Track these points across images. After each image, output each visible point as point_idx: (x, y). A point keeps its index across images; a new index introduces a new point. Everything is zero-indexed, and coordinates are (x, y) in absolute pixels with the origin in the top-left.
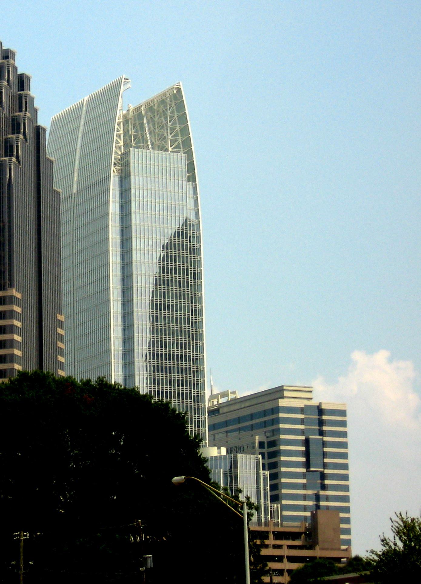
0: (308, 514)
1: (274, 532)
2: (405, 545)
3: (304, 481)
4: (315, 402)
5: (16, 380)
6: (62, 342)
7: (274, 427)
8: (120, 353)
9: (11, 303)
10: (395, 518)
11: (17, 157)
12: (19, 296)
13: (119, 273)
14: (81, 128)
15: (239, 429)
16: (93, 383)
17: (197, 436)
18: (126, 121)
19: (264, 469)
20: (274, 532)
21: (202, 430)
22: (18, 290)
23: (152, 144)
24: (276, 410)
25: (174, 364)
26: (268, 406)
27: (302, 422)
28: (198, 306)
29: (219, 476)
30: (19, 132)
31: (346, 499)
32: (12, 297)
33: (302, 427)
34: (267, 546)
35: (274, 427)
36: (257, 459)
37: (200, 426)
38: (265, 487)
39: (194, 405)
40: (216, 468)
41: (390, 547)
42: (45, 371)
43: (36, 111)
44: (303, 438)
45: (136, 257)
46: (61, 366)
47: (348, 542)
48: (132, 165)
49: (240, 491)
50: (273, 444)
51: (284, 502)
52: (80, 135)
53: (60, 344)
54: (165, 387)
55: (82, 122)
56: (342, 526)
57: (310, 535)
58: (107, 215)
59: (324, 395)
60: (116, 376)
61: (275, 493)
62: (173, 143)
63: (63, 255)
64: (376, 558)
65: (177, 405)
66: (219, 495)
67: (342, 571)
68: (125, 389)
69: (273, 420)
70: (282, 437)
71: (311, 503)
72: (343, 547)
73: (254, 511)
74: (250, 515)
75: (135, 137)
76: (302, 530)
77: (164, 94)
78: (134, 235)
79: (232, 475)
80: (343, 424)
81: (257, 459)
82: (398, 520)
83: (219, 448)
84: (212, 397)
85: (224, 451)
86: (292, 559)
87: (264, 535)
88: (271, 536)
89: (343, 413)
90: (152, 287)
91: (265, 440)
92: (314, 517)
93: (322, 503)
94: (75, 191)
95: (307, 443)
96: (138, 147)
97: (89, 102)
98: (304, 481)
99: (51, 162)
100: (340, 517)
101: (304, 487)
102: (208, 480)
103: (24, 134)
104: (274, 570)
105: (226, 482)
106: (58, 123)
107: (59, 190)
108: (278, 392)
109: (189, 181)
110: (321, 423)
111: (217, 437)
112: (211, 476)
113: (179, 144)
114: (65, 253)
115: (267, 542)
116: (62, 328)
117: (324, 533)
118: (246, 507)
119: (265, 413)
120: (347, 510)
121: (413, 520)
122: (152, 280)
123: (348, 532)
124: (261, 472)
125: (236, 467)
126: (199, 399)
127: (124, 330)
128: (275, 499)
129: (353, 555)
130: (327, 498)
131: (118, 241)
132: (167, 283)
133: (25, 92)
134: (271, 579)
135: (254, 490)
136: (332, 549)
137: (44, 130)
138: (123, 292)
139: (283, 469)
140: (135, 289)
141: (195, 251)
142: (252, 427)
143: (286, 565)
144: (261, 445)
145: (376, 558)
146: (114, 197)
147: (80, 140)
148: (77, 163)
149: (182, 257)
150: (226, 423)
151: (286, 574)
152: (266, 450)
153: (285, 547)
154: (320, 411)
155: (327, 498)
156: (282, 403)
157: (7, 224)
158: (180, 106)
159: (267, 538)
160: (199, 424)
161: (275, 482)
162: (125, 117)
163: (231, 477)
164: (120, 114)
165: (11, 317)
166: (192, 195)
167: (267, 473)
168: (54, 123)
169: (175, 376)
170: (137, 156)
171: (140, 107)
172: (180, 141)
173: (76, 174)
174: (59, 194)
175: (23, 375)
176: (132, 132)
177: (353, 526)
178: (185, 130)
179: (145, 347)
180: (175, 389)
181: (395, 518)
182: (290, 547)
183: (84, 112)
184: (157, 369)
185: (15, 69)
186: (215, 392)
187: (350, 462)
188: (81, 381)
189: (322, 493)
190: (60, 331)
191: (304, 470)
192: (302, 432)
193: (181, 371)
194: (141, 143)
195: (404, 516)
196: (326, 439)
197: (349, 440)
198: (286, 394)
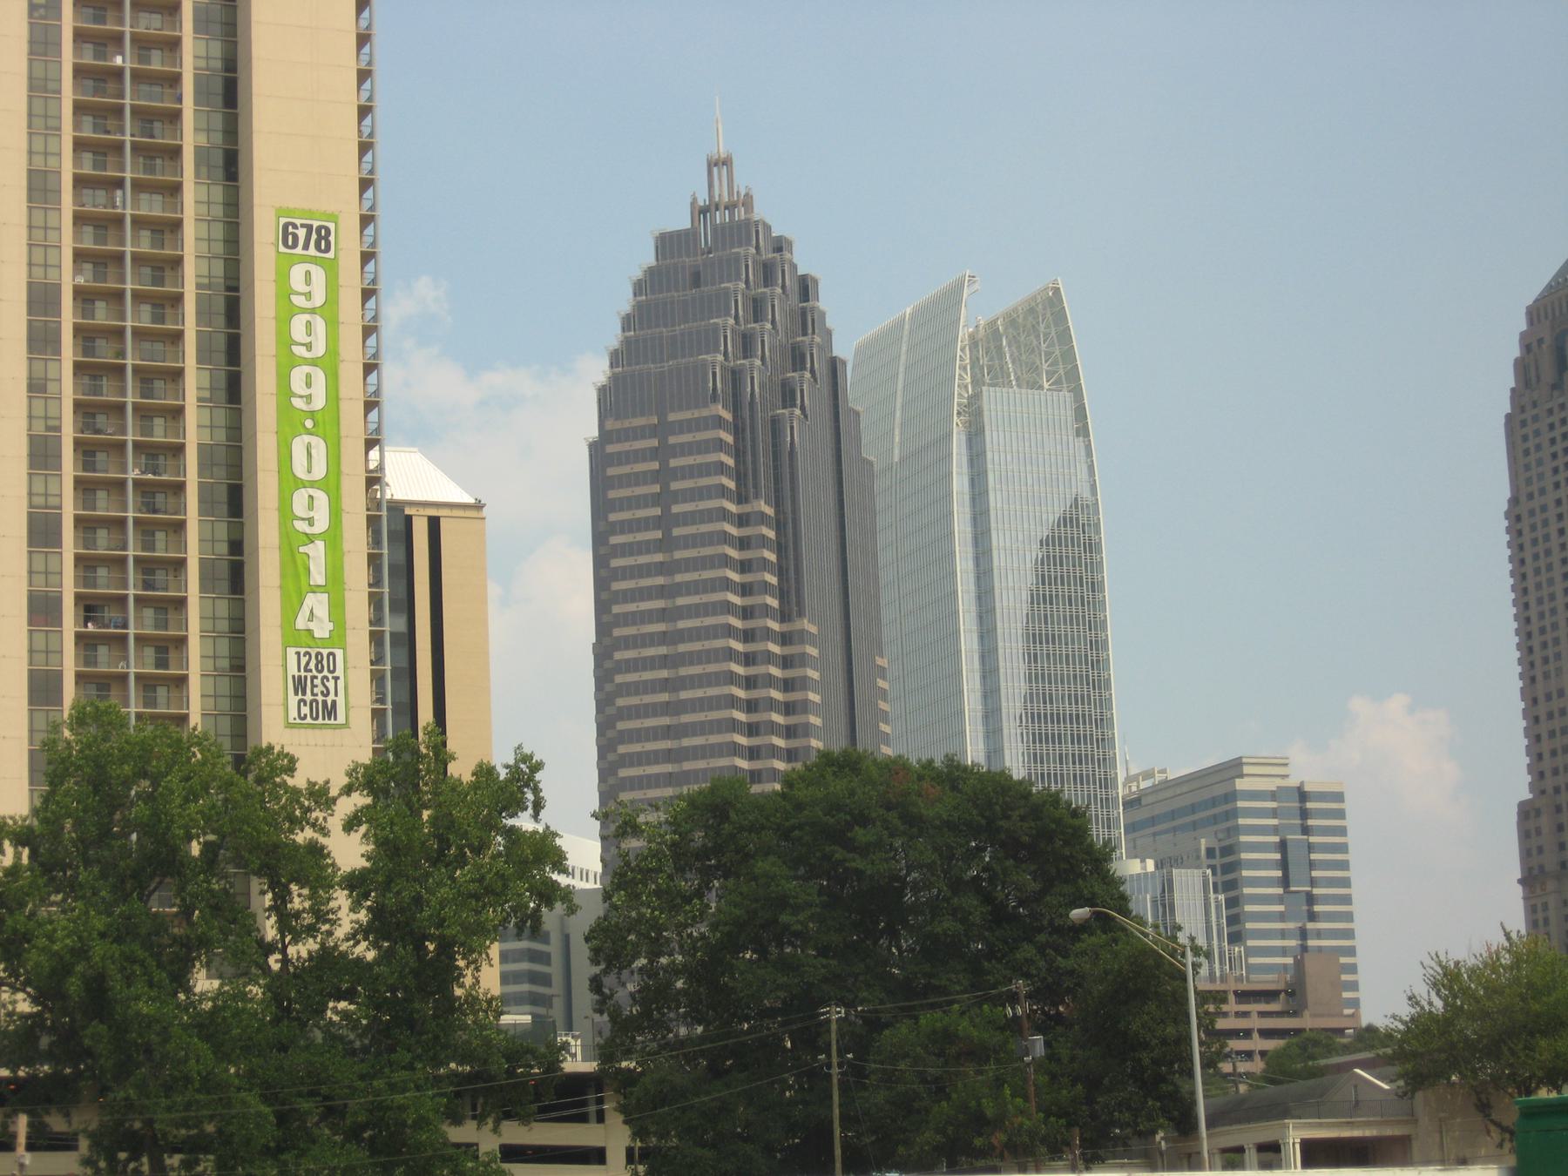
0: (1290, 960)
1: (1235, 992)
2: (1446, 1005)
3: (1281, 908)
4: (1293, 782)
5: (816, 765)
6: (885, 700)
7: (1229, 824)
8: (980, 715)
9: (802, 642)
10: (1428, 962)
11: (803, 408)
12: (813, 629)
13: (972, 587)
14: (903, 358)
15: (1175, 829)
16: (938, 764)
17: (1107, 843)
18: (974, 343)
19: (1216, 891)
20: (1235, 992)
21: (1115, 833)
22: (811, 621)
23: (1017, 379)
24: (1232, 796)
25: (1066, 729)
26: (1219, 790)
27: (1274, 813)
28: (1101, 635)
29: (1144, 905)
30: (803, 368)
31: (1349, 934)
32: (802, 631)
33: (1275, 822)
34: (1225, 1015)
35: (1229, 824)
36: (1205, 876)
37: (1109, 826)
38: (1218, 919)
39: (1101, 794)
40: (1140, 891)
41: (1422, 1008)
42: (860, 748)
43: (829, 333)
44: (1277, 839)
45: (999, 560)
46: (886, 738)
47: (1355, 1003)
48: (986, 413)
49: (1180, 928)
50: (1228, 850)
51: (1250, 943)
52: (901, 369)
53: (883, 705)
54: (1052, 767)
55: (904, 348)
56: (1344, 977)
57: (1294, 994)
58: (949, 494)
59: (1307, 770)
60: (974, 752)
61: (1235, 928)
62: (1050, 374)
63: (881, 562)
64: (1402, 1027)
65: (1073, 795)
66: (1146, 935)
67: (1346, 1049)
68: (989, 771)
69: (1227, 812)
70: (1243, 838)
71: (1293, 943)
72: (1347, 1011)
73: (1202, 959)
74: (1196, 966)
75: (989, 371)
76: (1281, 986)
77: (1034, 298)
78: (993, 525)
79: (1165, 903)
80: (1340, 814)
81: (1205, 876)
82: (1433, 964)
83: (1143, 861)
84: (1129, 779)
85: (1150, 865)
86: (1266, 1034)
87: (1219, 997)
88: (1232, 998)
89: (1339, 797)
90: (1025, 608)
91: (1216, 845)
92: (1299, 964)
93: (1311, 943)
94: (896, 459)
95: (1283, 846)
96: (994, 385)
97: (914, 316)
98: (1281, 908)
99: (857, 414)
100: (1341, 964)
101: (1282, 917)
102: (1126, 912)
103: (812, 371)
104: (1238, 1053)
105: (1155, 916)
106: (868, 350)
107: (872, 458)
108: (1234, 768)
109: (1078, 435)
110: (1305, 814)
111: (1139, 842)
112: (1132, 905)
113: (1060, 378)
114: (885, 557)
115: (1225, 1008)
116: (884, 678)
117: (1315, 990)
118: (1189, 953)
119: (1214, 802)
120: (1351, 951)
121: (1457, 963)
122: (1025, 595)
123: (1354, 986)
124: (1212, 896)
125: (1171, 889)
126: (1108, 783)
127: (984, 677)
128: (1235, 938)
129: (1364, 1024)
130: (1319, 934)
131: (969, 536)
132: (1048, 600)
133: (811, 303)
134: (1235, 1068)
135: (1202, 925)
136: (1330, 1015)
137: (844, 363)
138: (980, 617)
139: (1247, 891)
140: (998, 611)
141: (1093, 547)
142: (1195, 826)
143: (1257, 1044)
144: (1210, 852)
145: (1402, 1027)
146: (960, 466)
147: (901, 377)
148: (898, 414)
149: (1071, 557)
150: (1153, 821)
151: (1257, 1058)
152: (1217, 861)
153: (1254, 1015)
154: (1303, 795)
155: (1319, 934)
156: (1241, 784)
157: (790, 516)
158: (1060, 317)
159: (1224, 1000)
160: (1110, 823)
161: (1234, 911)
162: (972, 336)
163: (1164, 906)
164: (964, 332)
165: (803, 665)
166: (1083, 458)
167: (1222, 897)
168: (860, 351)
169: (1068, 748)
170: (994, 401)
171: (995, 321)
172: (1061, 372)
173: (897, 432)
174: (871, 464)
175: (826, 758)
176: (984, 361)
177: (1362, 977)
178: (1069, 355)
179: (1019, 705)
180: (1069, 768)
181: (1428, 962)
182: (1262, 1014)
183: (906, 333)
184: (1038, 738)
185: (794, 267)
186: (1133, 771)
187: (1352, 874)
188: (919, 761)
189: (1310, 926)
190: (881, 683)
191: (1280, 891)
192: (1275, 830)
193: (1077, 739)
194: (999, 377)
195: (1443, 958)
196: (1312, 839)
197: (1350, 839)
198: (1246, 770)
